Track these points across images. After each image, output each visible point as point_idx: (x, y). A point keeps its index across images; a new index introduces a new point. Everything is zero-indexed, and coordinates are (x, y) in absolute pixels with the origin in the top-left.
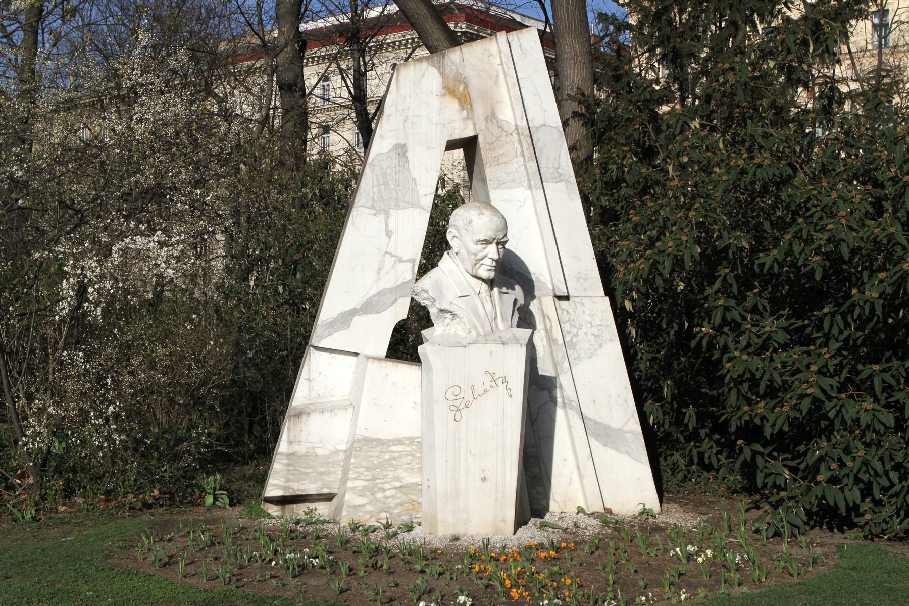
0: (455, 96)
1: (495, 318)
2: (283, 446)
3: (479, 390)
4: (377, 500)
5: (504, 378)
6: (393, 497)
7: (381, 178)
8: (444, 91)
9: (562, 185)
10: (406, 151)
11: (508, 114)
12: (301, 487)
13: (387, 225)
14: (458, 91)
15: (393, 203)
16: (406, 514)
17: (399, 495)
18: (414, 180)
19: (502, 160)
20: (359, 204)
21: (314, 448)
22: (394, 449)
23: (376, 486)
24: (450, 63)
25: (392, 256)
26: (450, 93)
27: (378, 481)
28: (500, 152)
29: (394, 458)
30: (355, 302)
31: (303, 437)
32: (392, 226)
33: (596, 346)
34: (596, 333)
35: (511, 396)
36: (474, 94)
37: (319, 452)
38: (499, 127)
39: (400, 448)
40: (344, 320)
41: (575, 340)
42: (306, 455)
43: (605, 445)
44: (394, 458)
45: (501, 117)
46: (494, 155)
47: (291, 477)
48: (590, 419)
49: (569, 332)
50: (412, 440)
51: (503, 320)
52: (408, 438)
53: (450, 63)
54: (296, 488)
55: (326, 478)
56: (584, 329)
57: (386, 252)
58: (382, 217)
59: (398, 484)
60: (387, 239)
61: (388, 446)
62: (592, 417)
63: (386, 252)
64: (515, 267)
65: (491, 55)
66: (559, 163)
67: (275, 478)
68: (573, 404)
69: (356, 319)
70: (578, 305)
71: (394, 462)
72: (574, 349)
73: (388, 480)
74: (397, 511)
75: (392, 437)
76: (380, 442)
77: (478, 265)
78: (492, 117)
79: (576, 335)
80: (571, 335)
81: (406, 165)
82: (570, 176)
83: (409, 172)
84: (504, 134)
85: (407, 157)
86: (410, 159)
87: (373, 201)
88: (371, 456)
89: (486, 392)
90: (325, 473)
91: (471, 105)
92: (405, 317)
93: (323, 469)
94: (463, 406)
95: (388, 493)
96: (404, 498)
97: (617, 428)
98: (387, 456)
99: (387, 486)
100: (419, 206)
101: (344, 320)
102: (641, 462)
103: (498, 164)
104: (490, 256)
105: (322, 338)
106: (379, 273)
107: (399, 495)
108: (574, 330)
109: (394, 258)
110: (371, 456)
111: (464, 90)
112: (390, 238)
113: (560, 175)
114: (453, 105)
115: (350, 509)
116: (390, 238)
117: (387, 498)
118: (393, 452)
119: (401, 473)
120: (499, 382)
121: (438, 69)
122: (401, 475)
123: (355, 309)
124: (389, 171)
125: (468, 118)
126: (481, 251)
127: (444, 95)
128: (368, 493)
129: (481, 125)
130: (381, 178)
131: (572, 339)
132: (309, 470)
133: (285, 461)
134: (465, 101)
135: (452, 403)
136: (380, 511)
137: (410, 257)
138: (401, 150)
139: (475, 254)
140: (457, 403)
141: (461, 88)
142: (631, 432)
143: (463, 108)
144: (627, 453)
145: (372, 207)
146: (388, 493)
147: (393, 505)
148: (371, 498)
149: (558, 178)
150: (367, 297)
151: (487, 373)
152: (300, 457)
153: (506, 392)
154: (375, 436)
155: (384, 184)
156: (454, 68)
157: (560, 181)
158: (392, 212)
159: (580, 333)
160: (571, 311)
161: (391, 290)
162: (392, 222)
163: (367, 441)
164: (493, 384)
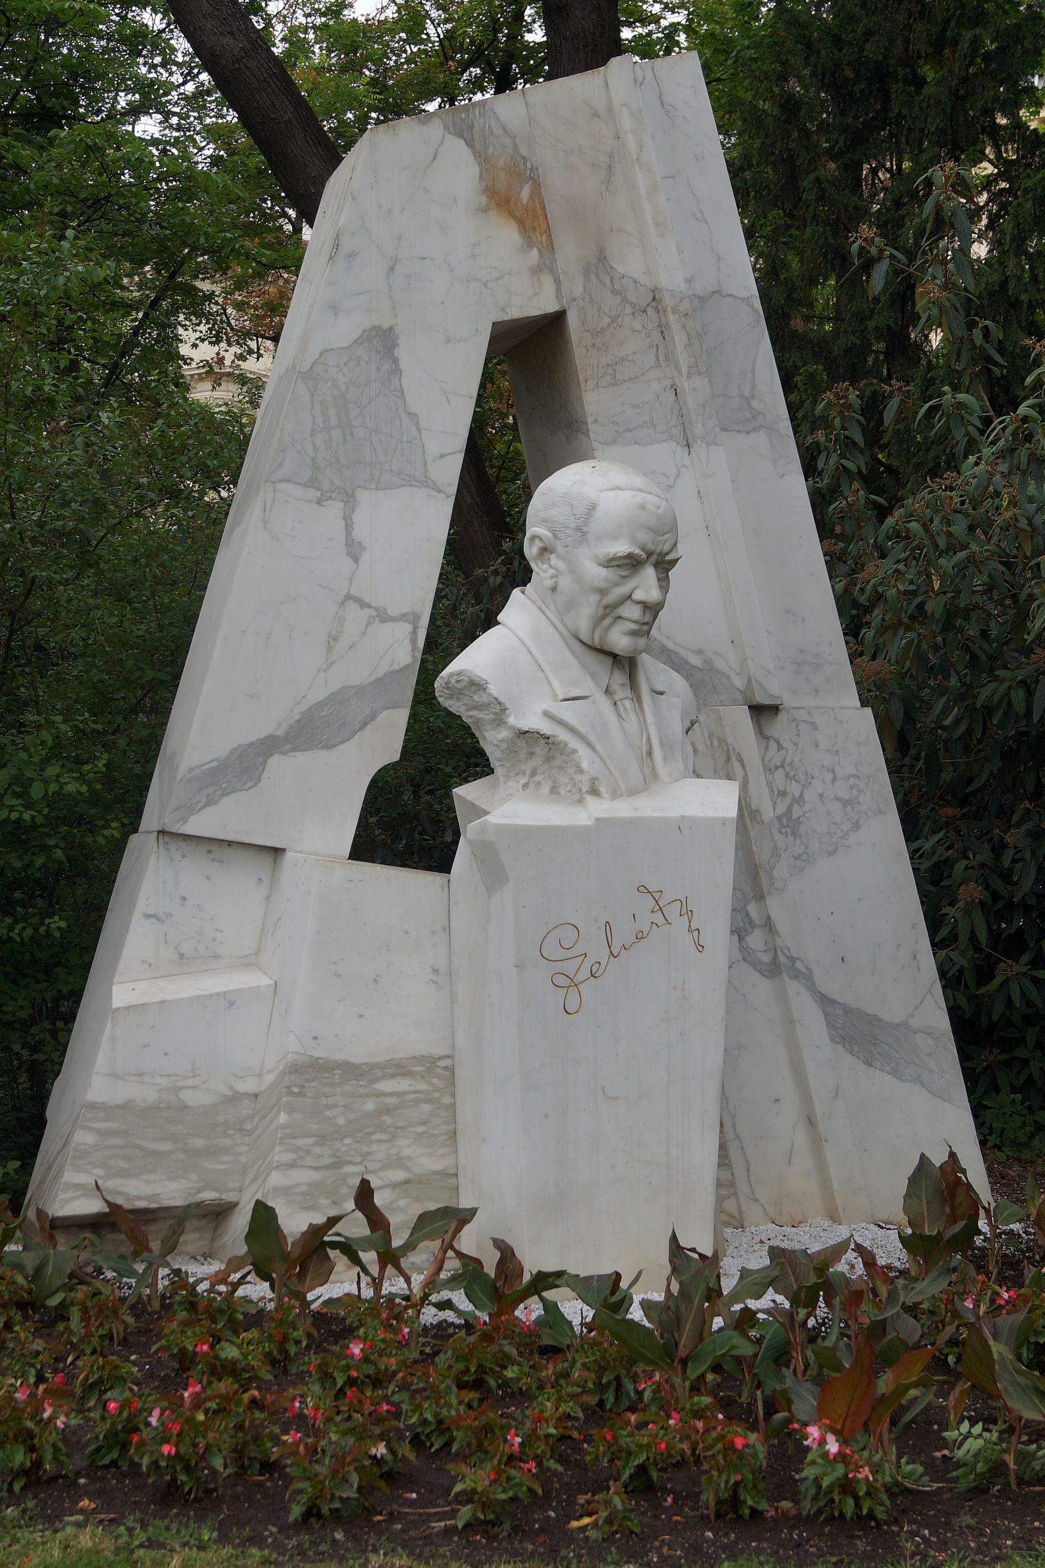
0: (512, 215)
1: (650, 753)
3: (622, 935)
5: (684, 903)
7: (332, 412)
8: (484, 200)
9: (760, 440)
10: (395, 345)
13: (349, 528)
14: (515, 196)
17: (402, 1203)
18: (414, 417)
22: (386, 1086)
25: (363, 604)
26: (499, 205)
29: (387, 1110)
32: (361, 531)
33: (846, 827)
34: (845, 794)
35: (700, 947)
36: (555, 210)
37: (190, 1098)
38: (615, 292)
39: (402, 1085)
40: (245, 765)
41: (796, 811)
45: (620, 268)
46: (604, 361)
50: (429, 1063)
51: (665, 759)
52: (421, 1059)
53: (497, 130)
54: (133, 1193)
55: (210, 1164)
56: (817, 785)
57: (348, 597)
58: (334, 510)
59: (399, 1175)
60: (349, 563)
61: (377, 1080)
63: (348, 597)
66: (753, 386)
69: (275, 762)
70: (803, 727)
71: (387, 1119)
72: (795, 834)
76: (351, 1070)
77: (608, 621)
78: (598, 264)
79: (800, 800)
80: (788, 801)
85: (395, 361)
86: (403, 364)
88: (329, 1107)
89: (640, 937)
90: (210, 1152)
92: (396, 757)
93: (199, 1143)
94: (585, 973)
97: (896, 1021)
98: (370, 1106)
100: (428, 483)
101: (245, 765)
103: (615, 383)
104: (638, 595)
106: (330, 649)
107: (402, 1203)
108: (795, 789)
109: (368, 612)
110: (329, 1107)
111: (531, 197)
112: (356, 560)
113: (756, 415)
114: (506, 235)
116: (356, 560)
119: (406, 1147)
120: (673, 912)
121: (470, 144)
122: (407, 1152)
123: (271, 737)
126: (616, 585)
127: (485, 210)
129: (575, 287)
130: (332, 412)
131: (790, 808)
132: (165, 1146)
134: (533, 222)
135: (559, 967)
139: (603, 592)
140: (570, 968)
141: (525, 194)
143: (529, 244)
144: (919, 1081)
145: (313, 483)
149: (749, 421)
150: (303, 708)
151: (643, 889)
153: (689, 938)
154: (339, 1057)
156: (508, 142)
157: (756, 430)
158: (361, 495)
159: (808, 795)
160: (785, 744)
161: (360, 690)
164: (658, 918)
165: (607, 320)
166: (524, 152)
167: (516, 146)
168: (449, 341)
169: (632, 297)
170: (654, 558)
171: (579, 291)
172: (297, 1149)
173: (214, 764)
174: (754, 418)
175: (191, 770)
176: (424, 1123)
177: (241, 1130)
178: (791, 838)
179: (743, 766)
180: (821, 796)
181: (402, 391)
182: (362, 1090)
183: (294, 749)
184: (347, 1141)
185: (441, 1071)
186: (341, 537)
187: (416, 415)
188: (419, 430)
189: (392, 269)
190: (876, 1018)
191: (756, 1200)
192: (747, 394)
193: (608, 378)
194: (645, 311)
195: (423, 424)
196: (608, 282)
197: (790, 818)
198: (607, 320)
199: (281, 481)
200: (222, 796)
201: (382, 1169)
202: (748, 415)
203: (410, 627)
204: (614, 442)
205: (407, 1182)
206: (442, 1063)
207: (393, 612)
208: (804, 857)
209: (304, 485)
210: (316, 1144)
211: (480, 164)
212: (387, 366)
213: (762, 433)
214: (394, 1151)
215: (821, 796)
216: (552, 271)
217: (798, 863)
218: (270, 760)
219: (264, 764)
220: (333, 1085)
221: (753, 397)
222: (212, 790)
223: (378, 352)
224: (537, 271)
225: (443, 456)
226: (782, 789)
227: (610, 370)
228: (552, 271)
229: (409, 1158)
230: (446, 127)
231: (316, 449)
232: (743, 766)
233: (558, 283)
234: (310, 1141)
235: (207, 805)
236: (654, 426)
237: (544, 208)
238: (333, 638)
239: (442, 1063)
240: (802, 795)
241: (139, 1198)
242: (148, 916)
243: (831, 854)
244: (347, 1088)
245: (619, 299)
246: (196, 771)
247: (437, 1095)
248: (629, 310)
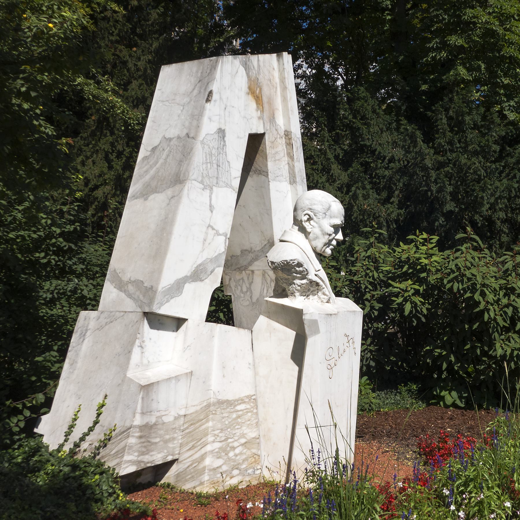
4: (229, 459)
6: (241, 454)
7: (208, 157)
8: (248, 90)
11: (280, 121)
13: (211, 200)
15: (215, 181)
16: (250, 468)
17: (245, 451)
20: (193, 178)
21: (161, 417)
22: (239, 408)
23: (228, 445)
24: (252, 68)
25: (213, 229)
27: (230, 440)
30: (186, 270)
32: (213, 202)
36: (265, 99)
37: (166, 419)
40: (178, 287)
42: (155, 424)
44: (239, 417)
47: (144, 449)
50: (249, 397)
52: (247, 397)
53: (252, 68)
59: (243, 441)
61: (235, 406)
65: (274, 69)
67: (129, 454)
69: (187, 286)
71: (239, 420)
73: (236, 438)
74: (244, 466)
75: (237, 397)
78: (272, 119)
82: (304, 179)
83: (226, 155)
85: (225, 142)
86: (227, 143)
87: (203, 177)
88: (223, 418)
93: (167, 437)
95: (237, 451)
96: (249, 453)
98: (234, 416)
99: (236, 444)
100: (231, 187)
101: (178, 287)
105: (161, 304)
106: (204, 244)
109: (215, 232)
110: (223, 418)
112: (212, 212)
115: (211, 473)
116: (212, 212)
117: (236, 455)
118: (238, 411)
119: (245, 430)
123: (186, 276)
124: (214, 152)
127: (249, 94)
128: (223, 454)
130: (208, 157)
132: (157, 440)
133: (137, 434)
136: (233, 469)
137: (224, 232)
139: (330, 235)
145: (202, 182)
146: (237, 451)
147: (241, 461)
148: (226, 458)
150: (195, 266)
152: (151, 427)
154: (225, 398)
162: (213, 196)
163: (220, 403)
165: (274, 139)
168: (238, 137)
171: (268, 128)
172: (215, 435)
173: (169, 286)
175: (163, 288)
176: (249, 420)
177: (180, 430)
181: (226, 153)
182: (232, 410)
183: (193, 281)
184: (229, 430)
185: (252, 400)
186: (209, 204)
200: (171, 298)
201: (239, 439)
203: (225, 238)
205: (246, 443)
206: (253, 398)
207: (221, 232)
210: (220, 433)
212: (222, 143)
214: (242, 432)
218: (186, 285)
219: (184, 286)
220: (224, 409)
224: (259, 118)
225: (235, 178)
228: (263, 119)
229: (246, 434)
233: (264, 123)
234: (219, 431)
235: (167, 302)
238: (205, 240)
239: (253, 398)
241: (148, 463)
242: (139, 346)
244: (228, 410)
246: (164, 289)
247: (252, 409)
248: (279, 137)
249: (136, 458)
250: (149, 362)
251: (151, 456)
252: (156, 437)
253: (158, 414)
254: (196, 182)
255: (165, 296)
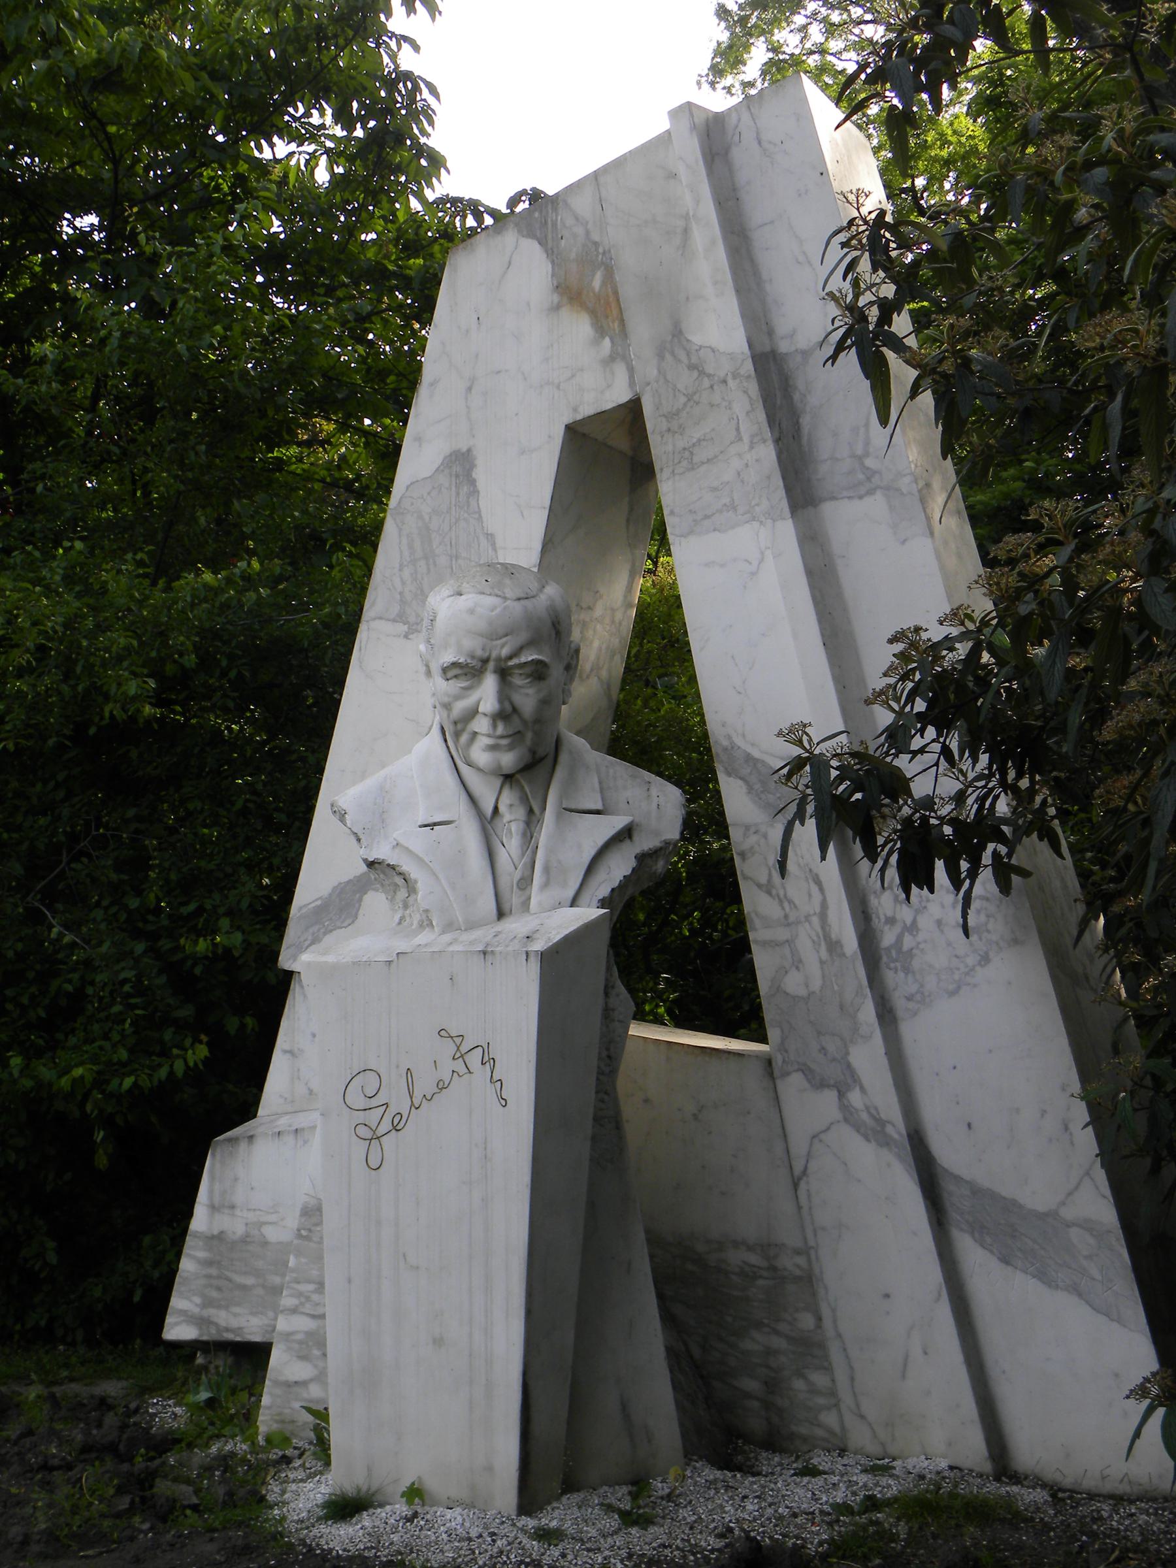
0: (583, 306)
2: (200, 1220)
8: (556, 298)
10: (472, 466)
12: (234, 1323)
18: (490, 537)
19: (701, 455)
28: (697, 434)
31: (239, 1197)
33: (971, 960)
36: (629, 291)
38: (692, 367)
42: (245, 1240)
43: (1005, 1260)
45: (697, 339)
47: (214, 1294)
48: (958, 1179)
49: (891, 921)
53: (570, 221)
54: (223, 1323)
62: (965, 1173)
64: (739, 741)
68: (889, 1129)
72: (907, 970)
78: (674, 339)
79: (913, 928)
80: (897, 929)
81: (473, 503)
84: (706, 382)
85: (473, 482)
86: (481, 485)
87: (403, 602)
91: (622, 322)
97: (1041, 1208)
102: (1119, 1320)
103: (692, 467)
105: (301, 949)
113: (870, 474)
114: (580, 327)
125: (612, 358)
126: (458, 698)
127: (557, 308)
129: (648, 370)
131: (899, 939)
132: (250, 1281)
133: (201, 1254)
138: (461, 465)
141: (597, 283)
142: (1087, 1226)
143: (601, 331)
144: (1076, 1290)
155: (426, 558)
156: (580, 231)
157: (871, 492)
166: (596, 237)
167: (588, 233)
168: (523, 453)
169: (709, 369)
170: (491, 665)
173: (319, 903)
174: (869, 479)
175: (301, 908)
178: (901, 975)
179: (821, 890)
180: (939, 923)
181: (479, 512)
187: (492, 535)
188: (495, 550)
189: (470, 389)
190: (1014, 1203)
191: (862, 1417)
192: (859, 452)
193: (685, 463)
194: (725, 382)
195: (499, 543)
196: (683, 357)
197: (899, 950)
198: (683, 399)
199: (374, 619)
200: (325, 934)
202: (861, 476)
204: (691, 532)
208: (918, 997)
209: (394, 621)
211: (553, 262)
213: (879, 495)
215: (939, 923)
216: (626, 358)
217: (911, 1005)
221: (867, 454)
222: (316, 928)
223: (457, 476)
226: (889, 914)
227: (687, 454)
228: (626, 358)
230: (519, 231)
231: (403, 583)
232: (821, 890)
233: (631, 370)
235: (313, 943)
236: (735, 509)
237: (616, 293)
240: (914, 921)
241: (227, 1330)
242: (285, 1052)
243: (953, 993)
245: (696, 374)
246: (304, 911)
249: (196, 1310)
250: (311, 1092)
251: (235, 1315)
252: (245, 1273)
253: (251, 1217)
254: (383, 622)
255: (307, 928)
